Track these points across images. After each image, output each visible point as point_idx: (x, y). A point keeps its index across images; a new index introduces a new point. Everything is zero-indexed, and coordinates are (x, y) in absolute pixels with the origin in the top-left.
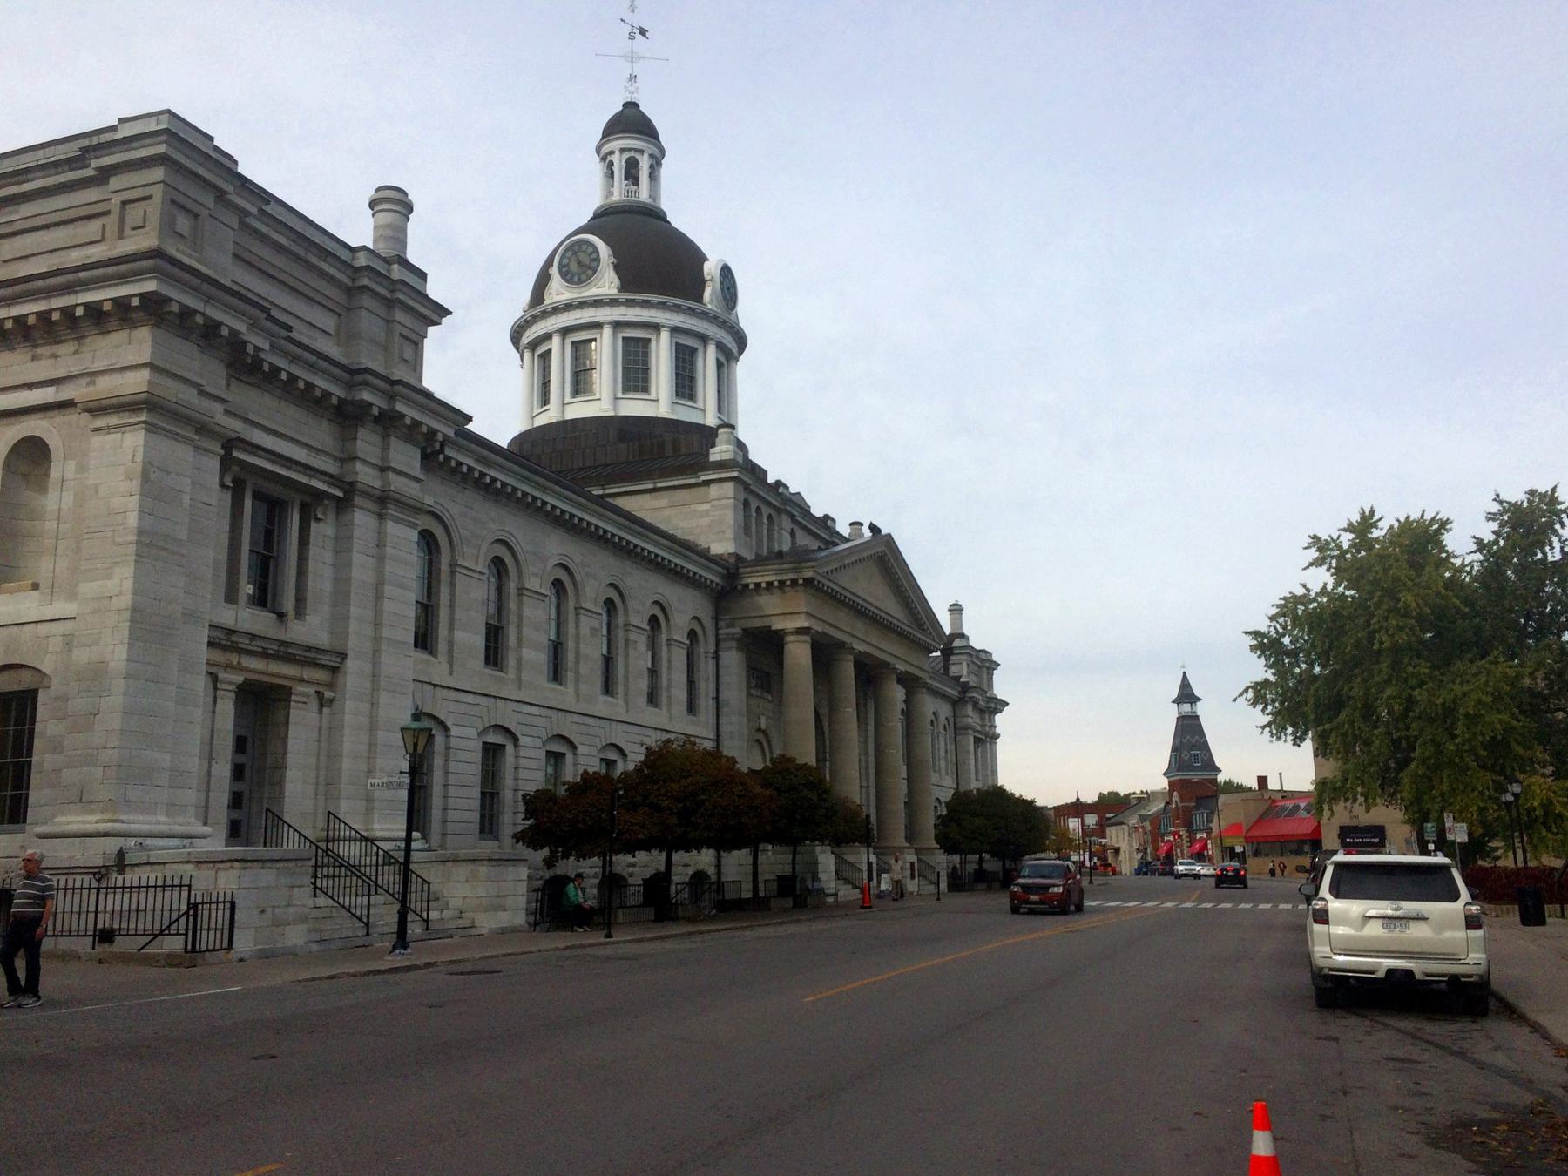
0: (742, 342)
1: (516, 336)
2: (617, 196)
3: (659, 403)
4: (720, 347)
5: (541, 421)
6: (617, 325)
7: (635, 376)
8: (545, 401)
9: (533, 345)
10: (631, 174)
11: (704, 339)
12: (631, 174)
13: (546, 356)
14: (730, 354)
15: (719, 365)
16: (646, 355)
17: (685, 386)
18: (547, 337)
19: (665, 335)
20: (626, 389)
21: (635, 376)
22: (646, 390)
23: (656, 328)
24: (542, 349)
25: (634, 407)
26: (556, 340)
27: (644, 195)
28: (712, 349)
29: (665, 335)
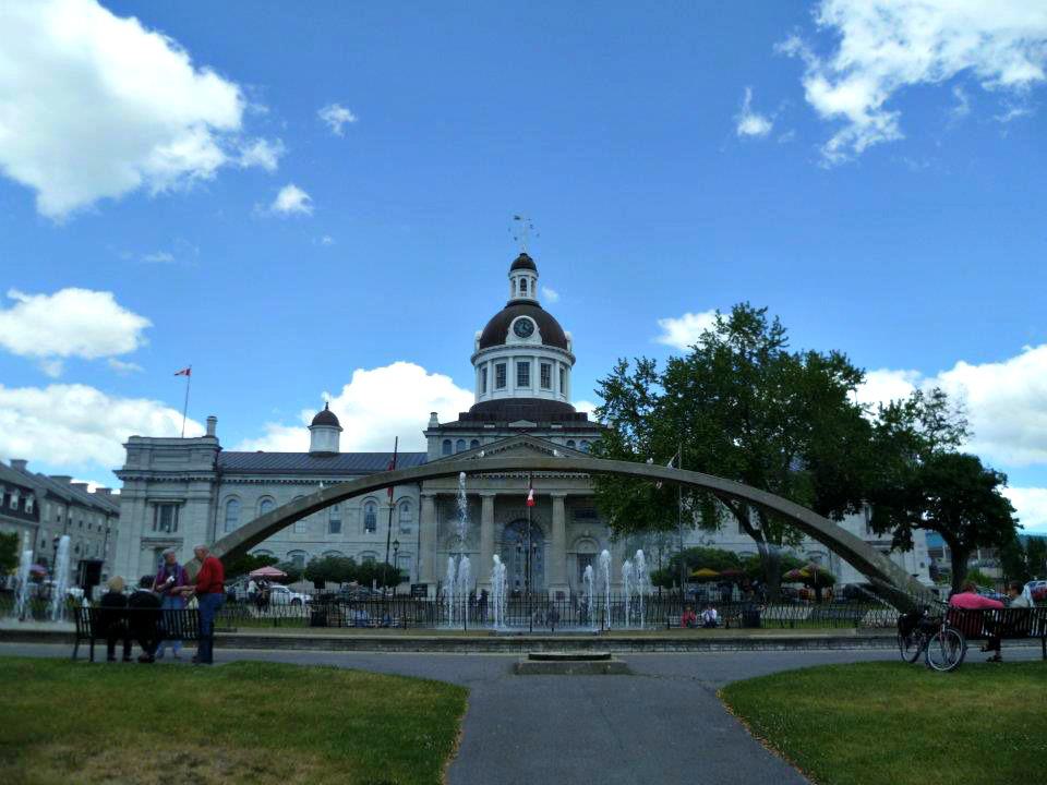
0: (573, 360)
1: (473, 360)
2: (518, 297)
3: (535, 391)
4: (561, 363)
5: (484, 399)
6: (515, 357)
7: (523, 379)
8: (485, 390)
9: (480, 365)
10: (523, 287)
11: (554, 361)
12: (523, 287)
13: (485, 371)
14: (565, 367)
15: (561, 371)
16: (528, 369)
17: (546, 381)
18: (486, 362)
19: (536, 360)
20: (520, 384)
21: (523, 379)
22: (528, 385)
23: (532, 357)
24: (483, 367)
25: (523, 394)
26: (489, 364)
27: (529, 296)
28: (558, 365)
29: (536, 360)
